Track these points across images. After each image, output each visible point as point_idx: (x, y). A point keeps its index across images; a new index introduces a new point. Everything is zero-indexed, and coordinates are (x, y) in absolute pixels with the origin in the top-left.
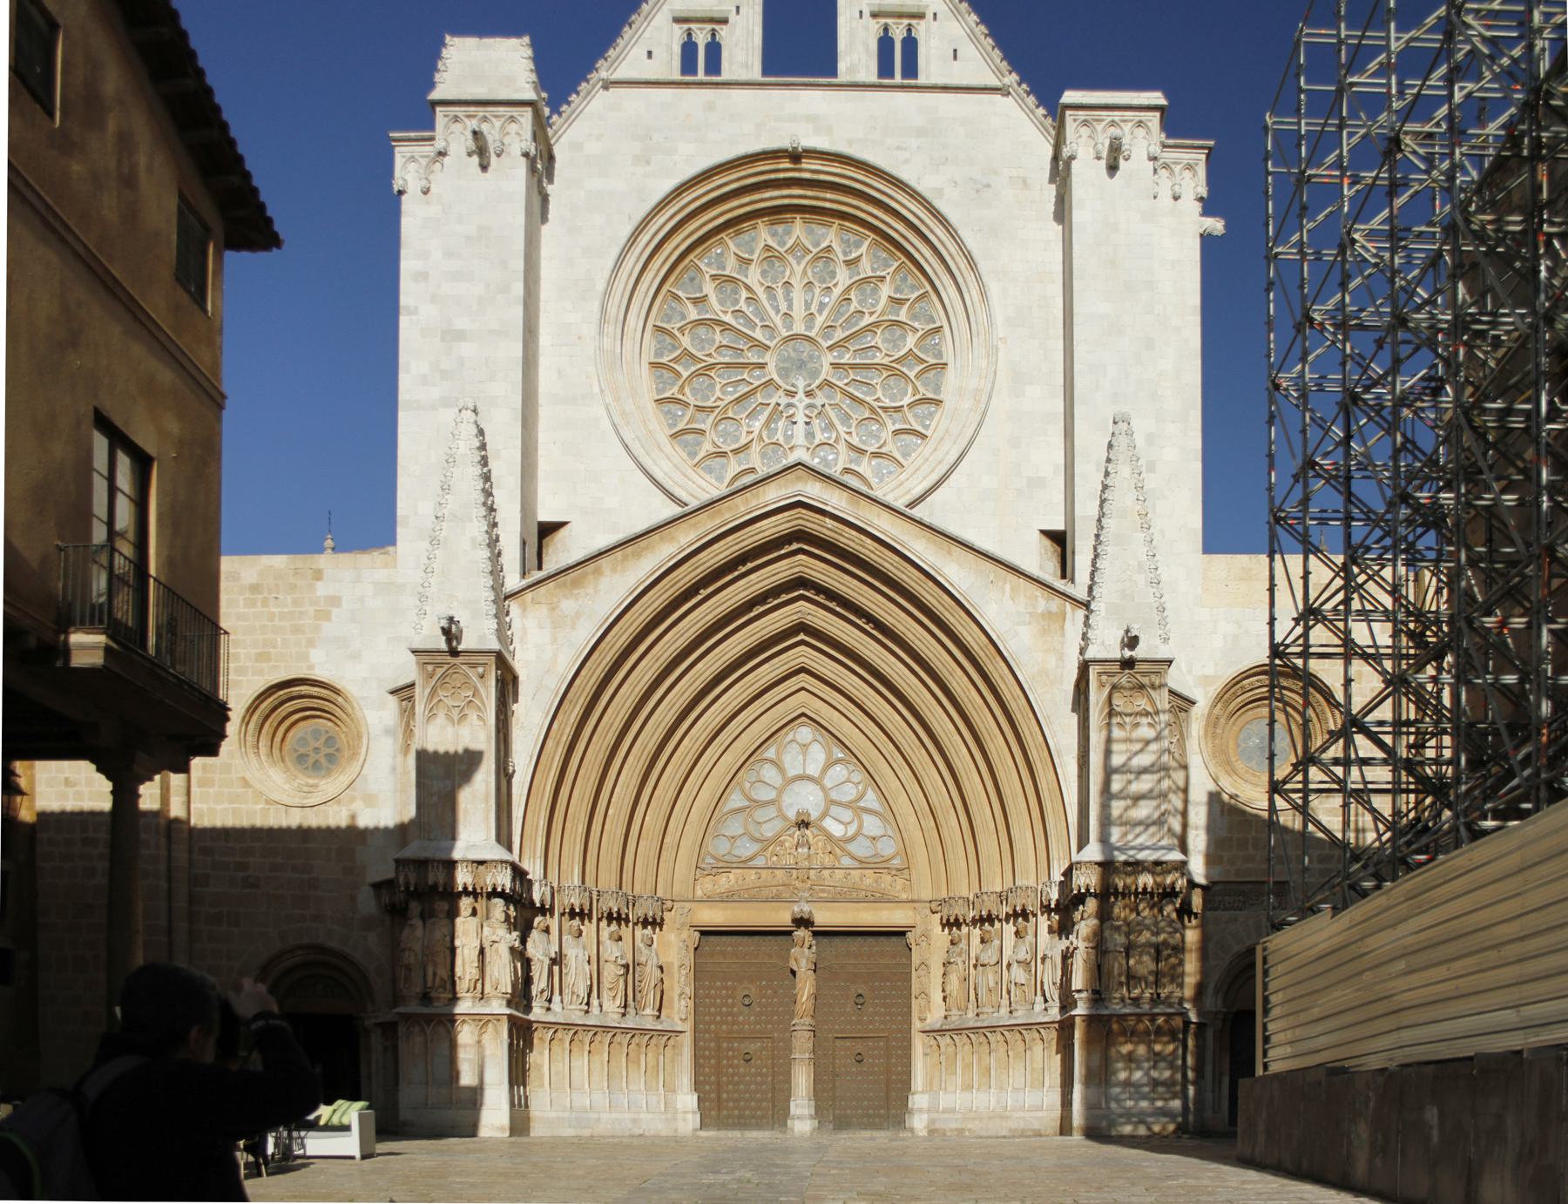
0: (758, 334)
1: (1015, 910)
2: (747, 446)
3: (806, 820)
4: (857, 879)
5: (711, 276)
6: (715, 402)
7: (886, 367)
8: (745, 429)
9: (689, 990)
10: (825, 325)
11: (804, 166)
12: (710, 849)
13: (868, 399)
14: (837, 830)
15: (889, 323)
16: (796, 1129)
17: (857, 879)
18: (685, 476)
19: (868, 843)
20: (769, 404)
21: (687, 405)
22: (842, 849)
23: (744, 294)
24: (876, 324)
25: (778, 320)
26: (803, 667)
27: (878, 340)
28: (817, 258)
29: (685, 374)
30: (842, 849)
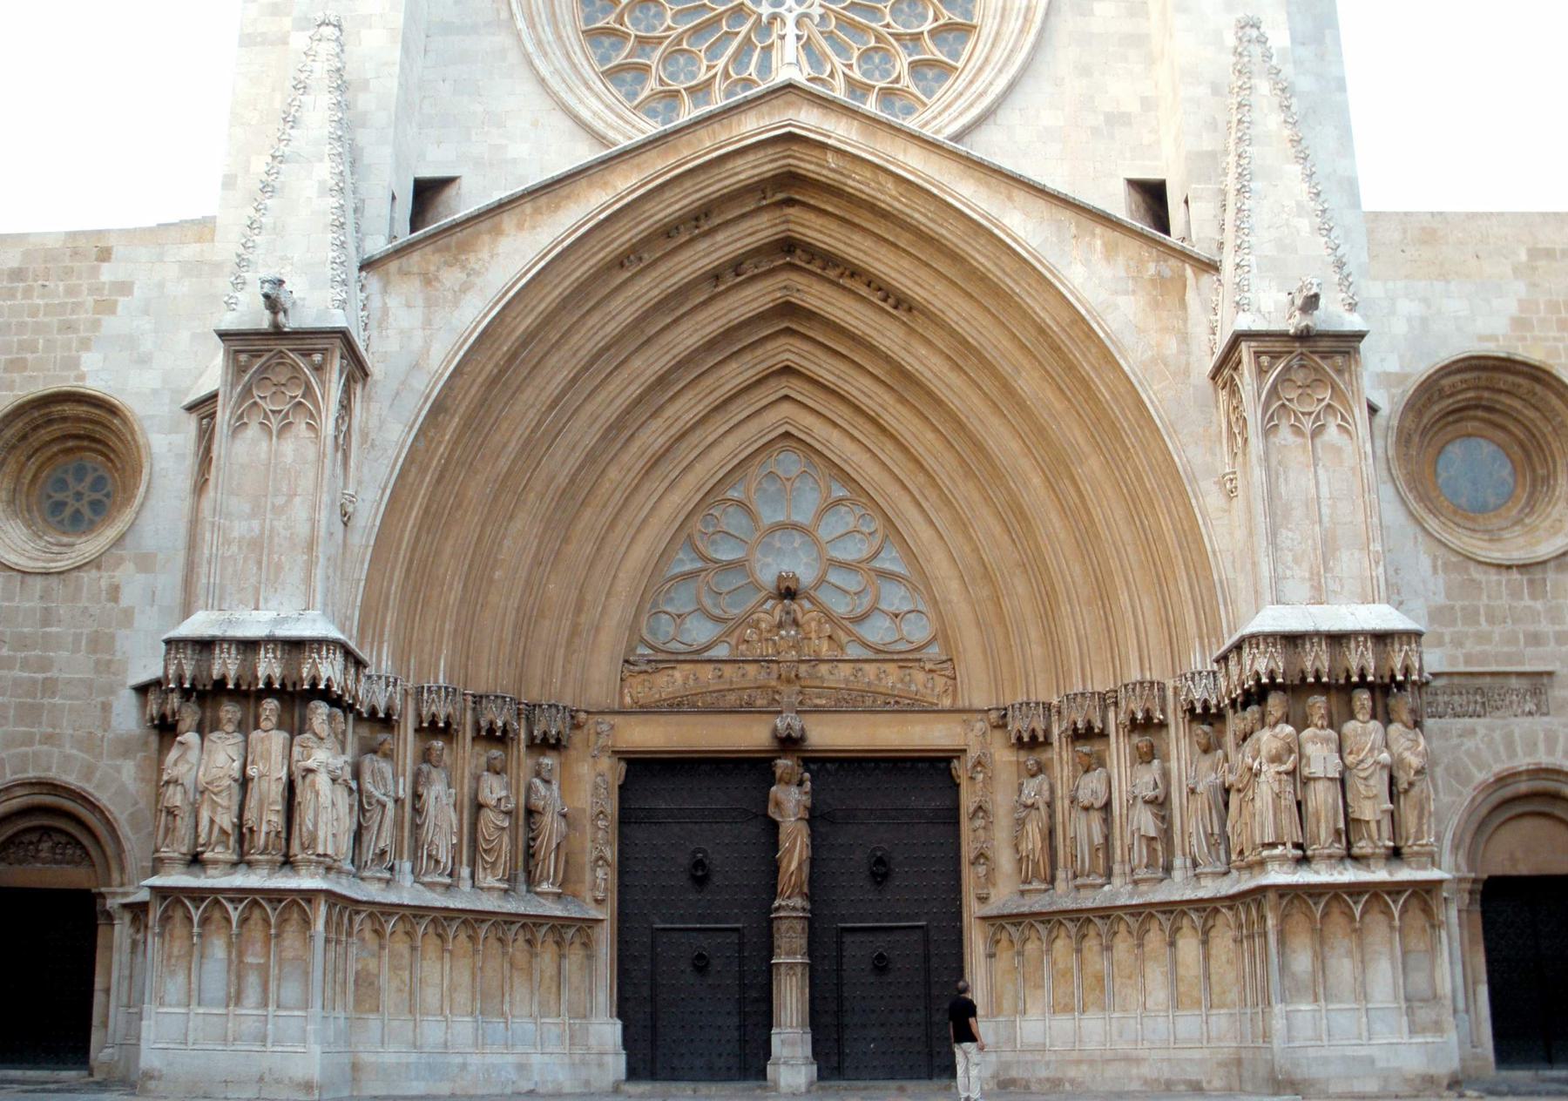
1: (1133, 720)
2: (708, 83)
3: (793, 586)
4: (872, 677)
6: (665, 31)
8: (705, 63)
9: (611, 853)
12: (647, 637)
13: (873, 25)
14: (840, 607)
16: (783, 1083)
17: (872, 677)
18: (621, 118)
19: (888, 623)
20: (737, 33)
21: (626, 36)
22: (849, 633)
26: (787, 367)
30: (849, 633)
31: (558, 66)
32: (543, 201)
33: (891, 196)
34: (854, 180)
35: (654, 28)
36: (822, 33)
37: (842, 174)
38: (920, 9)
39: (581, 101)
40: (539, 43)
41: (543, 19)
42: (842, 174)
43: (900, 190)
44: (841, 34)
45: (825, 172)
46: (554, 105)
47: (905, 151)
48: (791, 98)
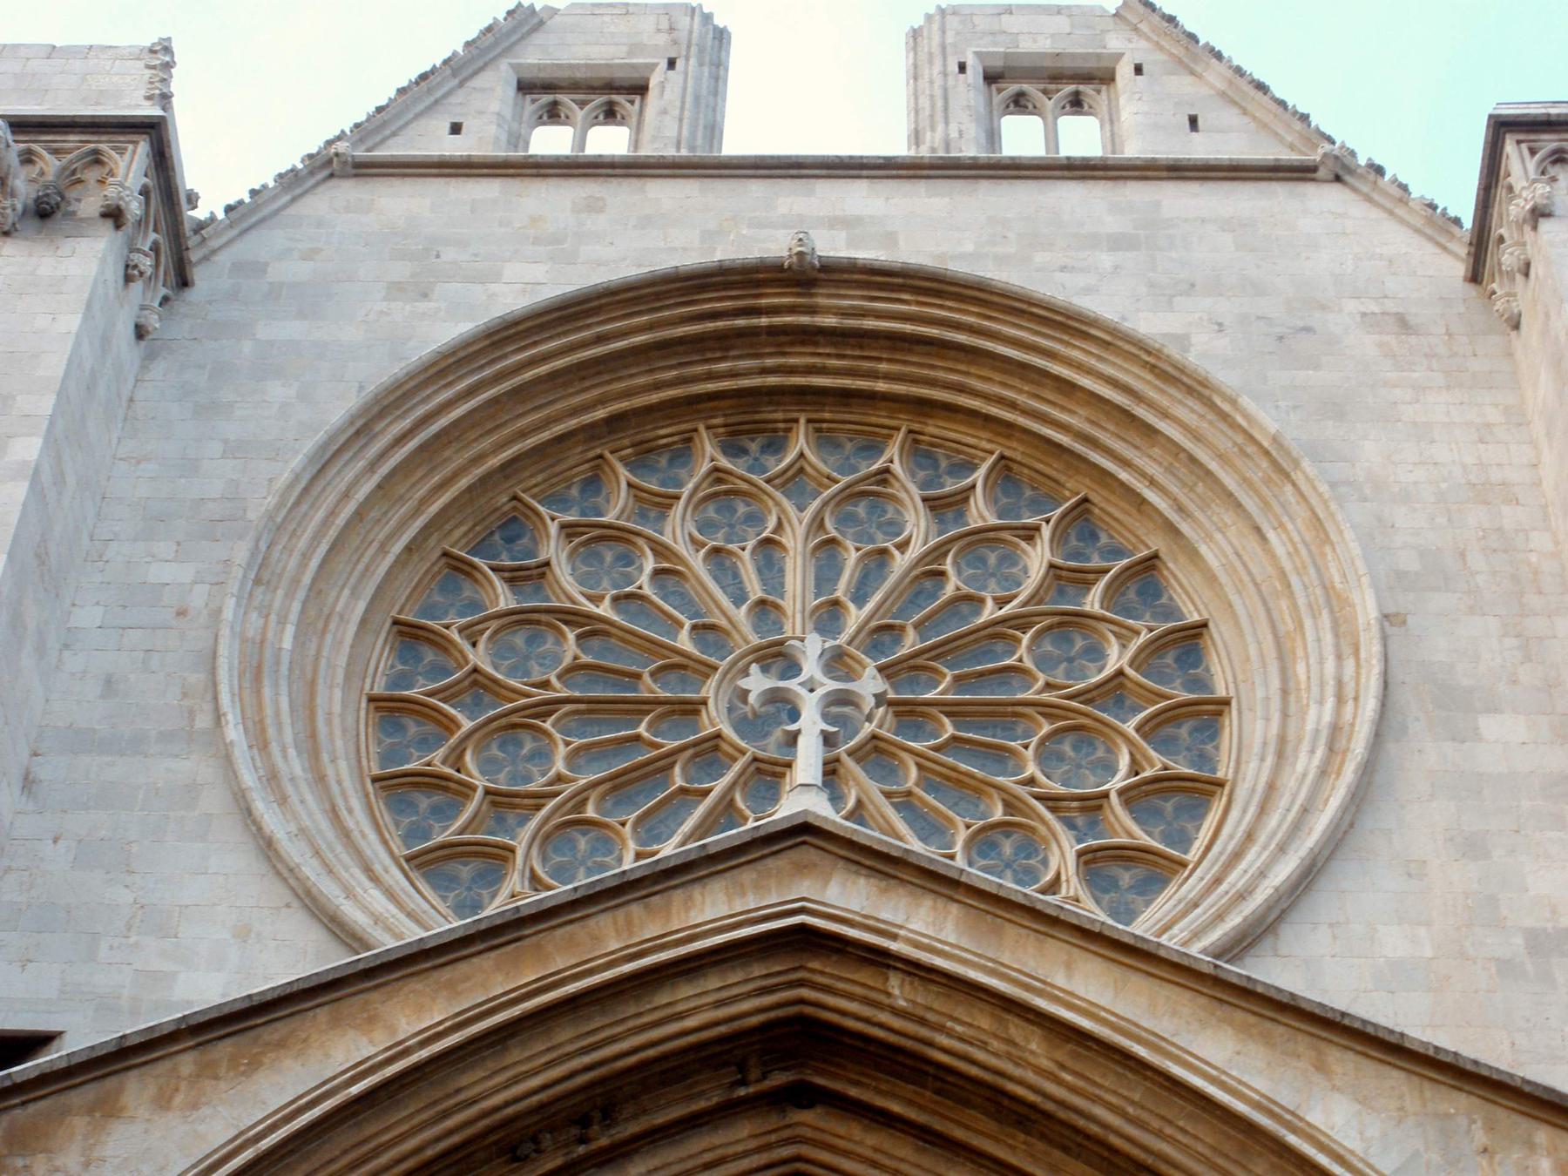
0: (684, 641)
5: (563, 526)
7: (1048, 711)
10: (874, 624)
11: (822, 301)
15: (1056, 619)
23: (650, 564)
24: (1020, 622)
25: (741, 614)
27: (1023, 654)
28: (851, 495)
29: (467, 725)
31: (307, 822)
32: (224, 1049)
33: (1039, 1071)
34: (950, 1034)
35: (528, 779)
36: (888, 795)
37: (922, 1021)
38: (1100, 753)
39: (350, 894)
40: (272, 778)
41: (285, 733)
42: (922, 1021)
43: (1060, 1055)
44: (930, 799)
45: (884, 1017)
46: (289, 897)
47: (1069, 966)
48: (807, 855)
